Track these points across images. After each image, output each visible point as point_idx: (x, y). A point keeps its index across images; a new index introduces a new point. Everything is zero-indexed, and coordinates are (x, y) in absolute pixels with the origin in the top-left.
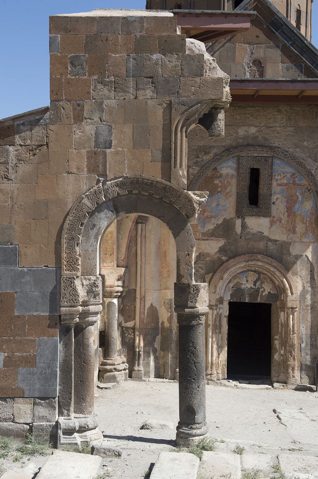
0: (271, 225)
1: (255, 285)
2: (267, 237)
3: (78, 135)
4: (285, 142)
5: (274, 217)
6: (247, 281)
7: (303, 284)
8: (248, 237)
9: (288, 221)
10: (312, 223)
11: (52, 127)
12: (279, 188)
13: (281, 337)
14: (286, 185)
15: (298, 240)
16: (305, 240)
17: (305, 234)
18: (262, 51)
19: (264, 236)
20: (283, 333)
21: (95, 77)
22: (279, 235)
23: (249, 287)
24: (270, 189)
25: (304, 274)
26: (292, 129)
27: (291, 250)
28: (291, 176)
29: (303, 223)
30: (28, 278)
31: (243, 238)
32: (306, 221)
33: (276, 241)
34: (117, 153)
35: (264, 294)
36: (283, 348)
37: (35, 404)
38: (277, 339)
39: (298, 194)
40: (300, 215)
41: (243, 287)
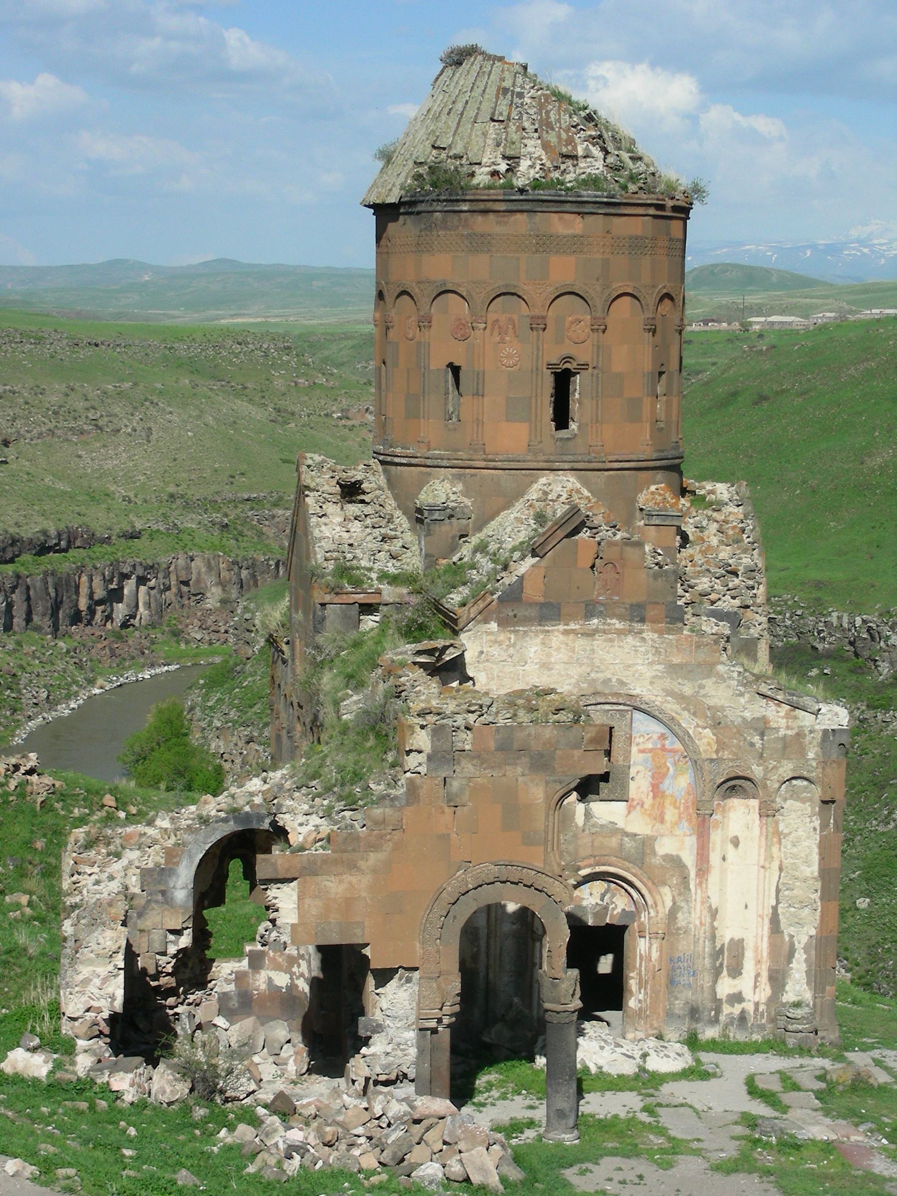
0: (629, 813)
1: (602, 900)
2: (623, 830)
4: (651, 688)
5: (633, 800)
6: (591, 894)
7: (674, 897)
8: (593, 830)
9: (653, 806)
10: (688, 808)
12: (642, 755)
13: (640, 974)
14: (651, 750)
15: (667, 833)
16: (678, 833)
17: (677, 824)
19: (618, 829)
20: (643, 969)
22: (639, 825)
23: (594, 903)
24: (627, 757)
25: (675, 882)
27: (657, 848)
28: (659, 738)
29: (675, 807)
31: (587, 832)
32: (680, 804)
33: (636, 835)
35: (615, 912)
36: (642, 991)
38: (633, 978)
39: (668, 764)
40: (672, 796)
41: (584, 903)
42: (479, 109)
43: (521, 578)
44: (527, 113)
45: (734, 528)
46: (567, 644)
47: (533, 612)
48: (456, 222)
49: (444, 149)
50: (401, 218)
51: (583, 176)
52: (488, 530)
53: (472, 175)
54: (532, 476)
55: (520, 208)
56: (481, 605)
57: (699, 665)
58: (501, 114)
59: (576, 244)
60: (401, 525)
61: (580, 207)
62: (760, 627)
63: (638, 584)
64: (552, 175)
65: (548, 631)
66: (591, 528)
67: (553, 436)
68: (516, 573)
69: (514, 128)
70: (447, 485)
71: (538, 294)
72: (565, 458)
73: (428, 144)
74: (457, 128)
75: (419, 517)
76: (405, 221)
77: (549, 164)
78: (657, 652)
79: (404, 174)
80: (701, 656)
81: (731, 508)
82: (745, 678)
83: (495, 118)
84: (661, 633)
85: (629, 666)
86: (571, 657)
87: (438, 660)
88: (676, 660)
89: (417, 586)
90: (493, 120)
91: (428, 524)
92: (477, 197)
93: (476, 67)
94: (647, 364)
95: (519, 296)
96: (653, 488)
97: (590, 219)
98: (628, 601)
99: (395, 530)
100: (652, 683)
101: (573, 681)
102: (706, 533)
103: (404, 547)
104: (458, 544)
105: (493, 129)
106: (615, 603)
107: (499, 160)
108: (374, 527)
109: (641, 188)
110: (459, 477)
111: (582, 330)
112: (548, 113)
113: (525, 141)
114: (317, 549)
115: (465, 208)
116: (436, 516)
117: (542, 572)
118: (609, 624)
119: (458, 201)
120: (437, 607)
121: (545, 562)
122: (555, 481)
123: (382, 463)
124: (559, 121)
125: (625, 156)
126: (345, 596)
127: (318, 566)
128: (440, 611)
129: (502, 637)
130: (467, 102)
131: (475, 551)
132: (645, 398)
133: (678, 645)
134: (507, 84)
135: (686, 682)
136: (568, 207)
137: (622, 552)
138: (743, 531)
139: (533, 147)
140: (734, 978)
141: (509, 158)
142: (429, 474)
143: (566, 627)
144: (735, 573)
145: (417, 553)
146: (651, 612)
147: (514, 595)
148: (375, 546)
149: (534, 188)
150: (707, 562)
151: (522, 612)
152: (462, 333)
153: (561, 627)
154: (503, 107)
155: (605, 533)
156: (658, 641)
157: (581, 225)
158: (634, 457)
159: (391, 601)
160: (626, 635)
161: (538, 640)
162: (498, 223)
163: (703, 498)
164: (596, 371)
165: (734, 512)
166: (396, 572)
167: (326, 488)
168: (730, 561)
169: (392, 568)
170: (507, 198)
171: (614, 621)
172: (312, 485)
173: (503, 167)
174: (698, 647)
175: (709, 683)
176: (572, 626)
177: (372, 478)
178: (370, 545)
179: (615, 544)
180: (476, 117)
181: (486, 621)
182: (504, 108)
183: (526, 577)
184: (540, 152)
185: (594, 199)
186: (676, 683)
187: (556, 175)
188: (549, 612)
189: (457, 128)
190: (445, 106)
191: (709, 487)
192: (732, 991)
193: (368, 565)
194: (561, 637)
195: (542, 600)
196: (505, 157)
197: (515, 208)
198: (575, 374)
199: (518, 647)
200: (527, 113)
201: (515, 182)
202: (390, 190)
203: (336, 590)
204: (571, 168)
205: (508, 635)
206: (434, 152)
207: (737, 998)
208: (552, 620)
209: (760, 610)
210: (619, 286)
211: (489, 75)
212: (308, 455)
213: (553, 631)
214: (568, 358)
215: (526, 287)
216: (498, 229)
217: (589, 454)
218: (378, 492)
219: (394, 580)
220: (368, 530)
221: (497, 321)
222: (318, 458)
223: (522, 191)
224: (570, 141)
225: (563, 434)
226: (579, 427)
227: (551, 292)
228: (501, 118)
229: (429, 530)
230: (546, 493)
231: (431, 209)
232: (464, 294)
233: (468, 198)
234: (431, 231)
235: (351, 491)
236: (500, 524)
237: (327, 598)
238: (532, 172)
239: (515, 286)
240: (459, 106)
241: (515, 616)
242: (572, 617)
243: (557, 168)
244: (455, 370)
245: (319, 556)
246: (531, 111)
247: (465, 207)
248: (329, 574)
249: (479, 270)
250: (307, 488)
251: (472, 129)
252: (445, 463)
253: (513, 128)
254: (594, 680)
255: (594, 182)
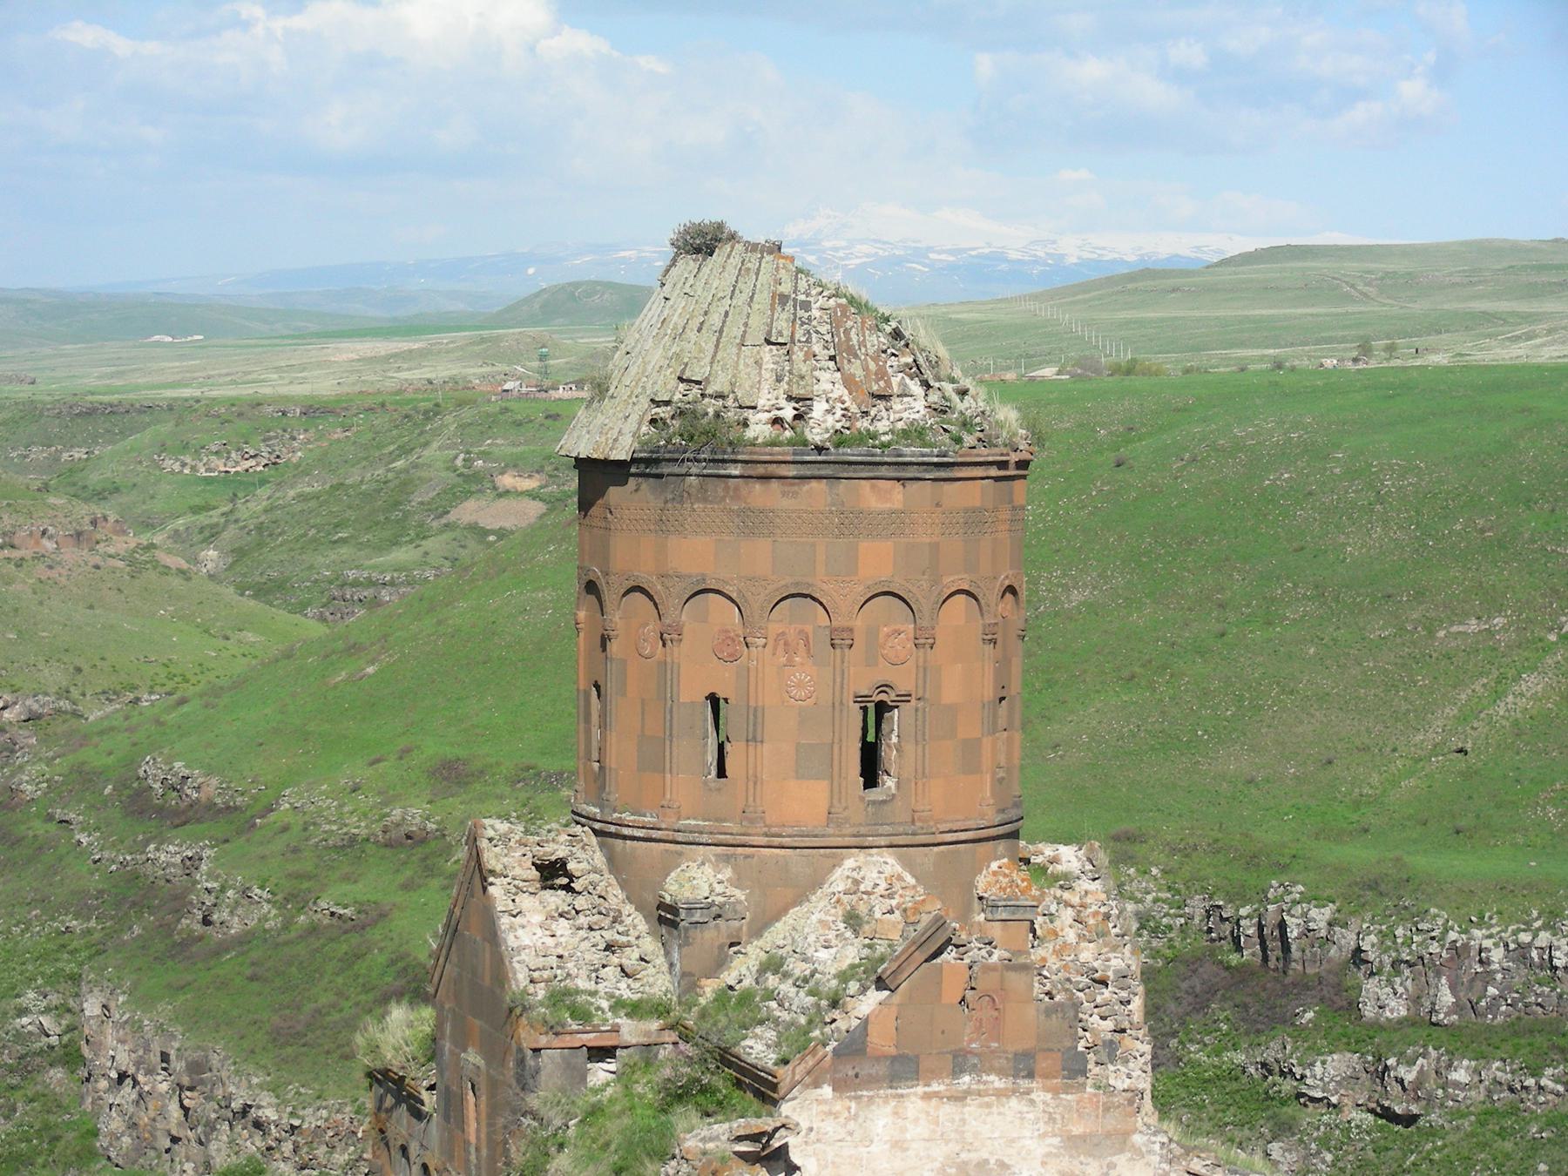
26: (1056, 1141)
42: (746, 325)
43: (865, 1022)
44: (817, 332)
45: (1095, 914)
46: (928, 1113)
47: (881, 1069)
48: (721, 492)
49: (698, 383)
50: (632, 482)
51: (900, 425)
52: (777, 934)
53: (745, 424)
54: (834, 856)
55: (817, 473)
56: (810, 1061)
57: (1108, 1135)
58: (780, 334)
59: (893, 523)
60: (635, 927)
61: (901, 471)
62: (1142, 1060)
63: (1025, 1023)
64: (858, 424)
65: (902, 1096)
66: (957, 946)
67: (862, 799)
68: (853, 1014)
69: (801, 354)
70: (708, 869)
71: (843, 595)
72: (881, 830)
73: (670, 376)
74: (716, 353)
75: (667, 917)
76: (639, 485)
77: (854, 409)
78: (1051, 1119)
79: (634, 418)
80: (1112, 1122)
81: (1085, 884)
82: (1170, 1151)
83: (773, 339)
84: (1056, 1092)
85: (1013, 1141)
86: (934, 1131)
87: (763, 1149)
88: (1077, 1130)
89: (670, 1021)
90: (769, 342)
91: (687, 930)
92: (755, 457)
93: (735, 261)
94: (989, 693)
95: (814, 599)
96: (994, 866)
97: (914, 487)
98: (1011, 1049)
99: (626, 934)
100: (1044, 1164)
101: (937, 1165)
102: (1057, 923)
103: (642, 959)
104: (727, 955)
105: (768, 353)
106: (992, 1052)
107: (783, 402)
108: (591, 929)
109: (980, 440)
110: (727, 859)
111: (901, 645)
112: (847, 332)
113: (817, 373)
114: (516, 965)
115: (736, 472)
116: (697, 917)
117: (894, 1011)
118: (985, 1083)
119: (724, 461)
120: (726, 1058)
121: (897, 998)
122: (867, 863)
123: (596, 832)
124: (862, 344)
125: (949, 388)
126: (568, 1037)
127: (525, 992)
128: (730, 1065)
129: (838, 1106)
130: (727, 313)
131: (764, 969)
132: (985, 740)
133: (1077, 1109)
134: (786, 288)
135: (1090, 1160)
136: (884, 471)
137: (1002, 980)
138: (1107, 917)
139: (828, 383)
141: (798, 400)
142: (680, 854)
143: (927, 1089)
144: (1104, 983)
145: (665, 968)
146: (1043, 1064)
147: (854, 1046)
148: (597, 957)
149: (837, 446)
150: (1065, 967)
151: (867, 1069)
152: (731, 649)
153: (920, 1089)
154: (782, 323)
155: (976, 952)
156: (1053, 1103)
157: (900, 497)
158: (971, 824)
159: (634, 1041)
160: (1008, 1097)
161: (889, 1109)
162: (784, 494)
163: (1042, 869)
164: (921, 704)
165: (1092, 890)
166: (636, 997)
167: (518, 871)
168: (1096, 964)
169: (625, 990)
170: (798, 458)
171: (992, 1077)
172: (499, 868)
173: (788, 413)
174: (1107, 1109)
175: (1121, 1160)
176: (935, 1087)
177: (580, 854)
178: (588, 957)
179: (993, 968)
180: (743, 336)
181: (817, 1084)
182: (784, 325)
183: (872, 1019)
184: (840, 391)
185: (921, 459)
186: (1076, 1162)
187: (863, 424)
188: (903, 1069)
189: (716, 353)
190: (692, 317)
191: (1049, 850)
193: (591, 986)
194: (920, 1104)
195: (893, 1051)
196: (790, 398)
197: (809, 473)
198: (891, 708)
199: (860, 1120)
200: (817, 332)
201: (809, 437)
202: (616, 440)
203: (556, 1030)
204: (884, 413)
205: (847, 1102)
206: (682, 386)
208: (907, 1079)
209: (1140, 1034)
210: (953, 581)
211: (757, 274)
212: (487, 822)
213: (908, 1095)
214: (884, 687)
215: (825, 587)
216: (786, 503)
217: (913, 822)
218: (595, 877)
219: (635, 1010)
220: (582, 933)
221: (783, 633)
222: (503, 827)
223: (820, 449)
224: (881, 374)
225: (874, 794)
226: (898, 785)
227: (860, 592)
228: (781, 340)
229: (687, 937)
230: (856, 882)
231: (683, 471)
232: (734, 596)
233: (740, 457)
234: (681, 502)
235: (552, 873)
236: (794, 929)
237: (543, 1041)
238: (830, 418)
239: (810, 585)
240: (715, 319)
241: (857, 1076)
242: (936, 1074)
243: (866, 413)
244: (714, 700)
245: (520, 976)
246: (824, 329)
247: (735, 470)
248: (541, 1004)
249: (756, 562)
250: (492, 872)
251: (738, 355)
252: (705, 838)
253: (799, 355)
254: (965, 1163)
255: (914, 433)
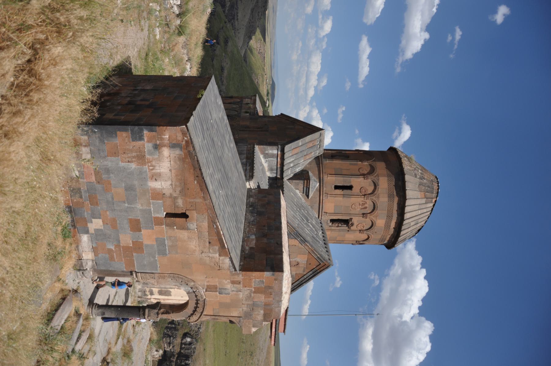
3: (226, 282)
11: (229, 272)
18: (303, 266)
21: (253, 290)
30: (152, 259)
34: (217, 296)
37: (93, 260)
140: (158, 292)
192: (154, 291)
207: (152, 293)
